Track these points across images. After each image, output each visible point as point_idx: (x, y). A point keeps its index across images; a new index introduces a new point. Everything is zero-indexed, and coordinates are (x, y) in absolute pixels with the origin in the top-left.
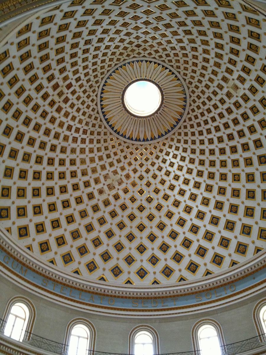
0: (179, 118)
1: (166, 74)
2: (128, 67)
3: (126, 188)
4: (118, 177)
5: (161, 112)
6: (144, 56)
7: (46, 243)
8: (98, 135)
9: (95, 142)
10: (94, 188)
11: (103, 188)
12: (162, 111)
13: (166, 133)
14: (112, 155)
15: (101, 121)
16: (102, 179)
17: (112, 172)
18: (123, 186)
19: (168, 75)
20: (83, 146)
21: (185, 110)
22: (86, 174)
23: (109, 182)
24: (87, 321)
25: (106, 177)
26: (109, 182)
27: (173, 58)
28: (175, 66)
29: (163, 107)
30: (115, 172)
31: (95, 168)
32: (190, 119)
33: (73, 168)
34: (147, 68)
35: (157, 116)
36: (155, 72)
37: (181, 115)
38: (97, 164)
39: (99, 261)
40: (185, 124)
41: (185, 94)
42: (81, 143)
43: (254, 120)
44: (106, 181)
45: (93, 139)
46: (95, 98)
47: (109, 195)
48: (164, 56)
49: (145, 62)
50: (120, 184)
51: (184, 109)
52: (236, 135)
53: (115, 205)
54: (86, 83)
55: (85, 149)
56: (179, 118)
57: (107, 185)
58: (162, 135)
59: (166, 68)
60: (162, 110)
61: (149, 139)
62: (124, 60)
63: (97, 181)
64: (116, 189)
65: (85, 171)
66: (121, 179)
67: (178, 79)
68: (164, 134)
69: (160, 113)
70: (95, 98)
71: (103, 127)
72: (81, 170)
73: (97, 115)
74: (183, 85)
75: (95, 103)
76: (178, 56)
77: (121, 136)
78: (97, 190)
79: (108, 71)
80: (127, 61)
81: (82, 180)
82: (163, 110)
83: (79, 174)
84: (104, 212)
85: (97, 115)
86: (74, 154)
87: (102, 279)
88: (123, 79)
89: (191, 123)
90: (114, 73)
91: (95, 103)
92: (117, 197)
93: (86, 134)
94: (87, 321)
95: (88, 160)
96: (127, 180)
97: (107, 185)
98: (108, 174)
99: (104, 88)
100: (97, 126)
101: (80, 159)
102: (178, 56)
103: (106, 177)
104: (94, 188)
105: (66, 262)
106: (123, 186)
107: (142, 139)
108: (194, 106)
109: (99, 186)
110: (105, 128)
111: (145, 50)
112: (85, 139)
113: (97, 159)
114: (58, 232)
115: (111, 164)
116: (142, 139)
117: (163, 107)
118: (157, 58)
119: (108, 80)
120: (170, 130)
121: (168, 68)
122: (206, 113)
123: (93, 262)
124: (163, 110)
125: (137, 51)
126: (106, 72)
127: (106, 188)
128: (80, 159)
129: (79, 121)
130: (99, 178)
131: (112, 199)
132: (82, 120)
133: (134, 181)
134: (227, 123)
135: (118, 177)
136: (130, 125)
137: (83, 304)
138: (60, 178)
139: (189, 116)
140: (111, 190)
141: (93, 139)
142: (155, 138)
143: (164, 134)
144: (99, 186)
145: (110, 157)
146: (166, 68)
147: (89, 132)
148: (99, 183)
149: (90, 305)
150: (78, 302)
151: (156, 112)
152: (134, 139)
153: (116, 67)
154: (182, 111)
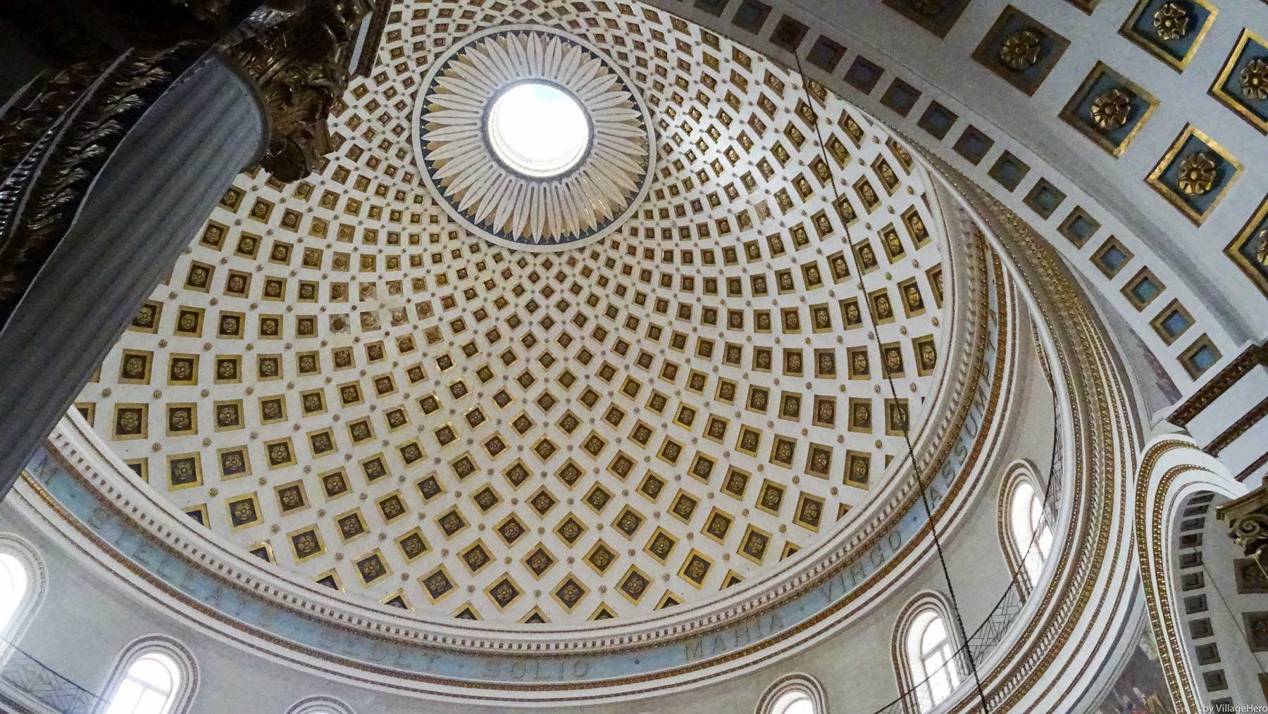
1: (619, 101)
2: (534, 42)
3: (410, 340)
4: (398, 301)
6: (584, 36)
7: (139, 411)
8: (386, 173)
9: (372, 188)
10: (323, 308)
11: (347, 315)
12: (575, 182)
13: (563, 240)
14: (404, 239)
15: (409, 140)
16: (354, 291)
17: (387, 283)
18: (404, 330)
19: (622, 105)
20: (336, 187)
21: (629, 205)
22: (315, 265)
23: (369, 305)
24: (182, 649)
25: (366, 290)
26: (369, 305)
27: (652, 74)
28: (648, 93)
30: (396, 287)
31: (348, 256)
33: (287, 236)
34: (581, 64)
35: (556, 188)
37: (617, 213)
38: (356, 248)
39: (268, 504)
41: (646, 169)
42: (332, 179)
43: (775, 303)
44: (362, 300)
45: (369, 180)
46: (417, 78)
47: (356, 339)
48: (632, 60)
49: (580, 49)
50: (396, 322)
51: (629, 202)
52: (723, 317)
53: (363, 372)
54: (410, 33)
55: (336, 196)
57: (362, 314)
58: (552, 241)
59: (626, 89)
61: (516, 235)
62: (532, 22)
63: (338, 292)
64: (382, 332)
65: (316, 255)
66: (405, 310)
68: (557, 238)
70: (417, 78)
71: (408, 158)
72: (307, 249)
73: (405, 124)
75: (412, 89)
76: (665, 76)
77: (446, 198)
78: (331, 316)
79: (479, 29)
81: (298, 277)
83: (297, 256)
84: (328, 380)
85: (405, 124)
86: (304, 201)
87: (262, 552)
90: (491, 40)
91: (412, 89)
92: (375, 353)
93: (356, 161)
94: (182, 649)
95: (334, 229)
96: (420, 319)
97: (362, 314)
98: (374, 284)
99: (451, 63)
100: (393, 151)
101: (315, 219)
102: (665, 76)
103: (366, 290)
104: (323, 308)
105: (176, 479)
106: (404, 330)
108: (655, 205)
109: (339, 308)
110: (413, 163)
111: (592, 22)
112: (348, 172)
113: (359, 235)
114: (182, 394)
115: (393, 263)
118: (615, 55)
119: (468, 50)
120: (577, 235)
121: (629, 90)
122: (676, 233)
123: (250, 501)
125: (572, 17)
126: (472, 28)
127: (355, 320)
128: (315, 219)
129: (352, 119)
130: (346, 285)
131: (360, 354)
132: (359, 119)
133: (436, 328)
134: (714, 281)
135: (398, 301)
137: (188, 602)
138: (240, 250)
139: (634, 223)
140: (368, 330)
141: (369, 180)
142: (530, 241)
143: (557, 238)
144: (339, 308)
145: (397, 242)
146: (626, 89)
147: (365, 157)
148: (341, 301)
149: (205, 611)
150: (174, 594)
151: (560, 178)
152: (478, 220)
153: (503, 28)
154: (624, 204)
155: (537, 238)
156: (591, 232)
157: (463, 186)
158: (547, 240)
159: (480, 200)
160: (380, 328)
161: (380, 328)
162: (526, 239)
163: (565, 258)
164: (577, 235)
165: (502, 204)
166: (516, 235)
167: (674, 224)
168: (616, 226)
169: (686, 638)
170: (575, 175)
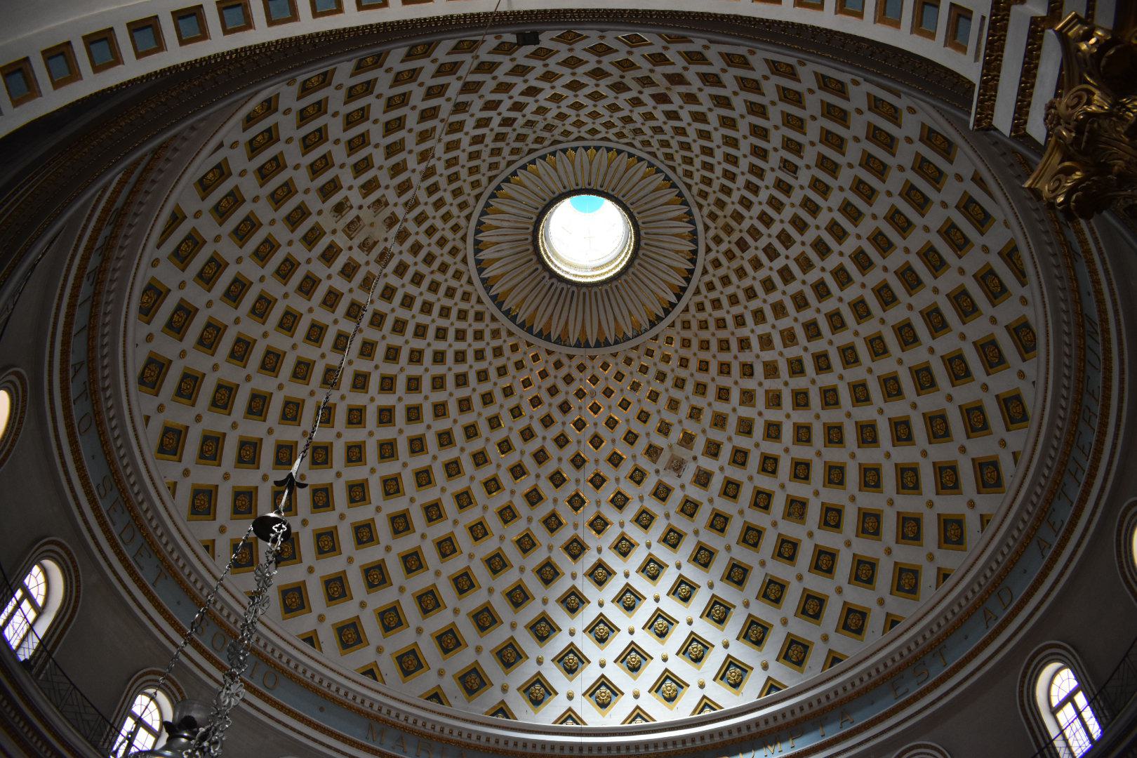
0: (554, 337)
5: (557, 288)
11: (351, 207)
13: (507, 313)
29: (568, 289)
32: (558, 365)
34: (677, 252)
35: (544, 278)
36: (663, 267)
40: (543, 356)
41: (616, 342)
44: (369, 207)
56: (554, 337)
58: (499, 305)
60: (563, 289)
64: (350, 243)
66: (375, 243)
67: (652, 324)
68: (505, 307)
69: (552, 284)
74: (638, 335)
80: (695, 210)
82: (561, 292)
88: (642, 194)
89: (551, 371)
97: (358, 217)
98: (387, 204)
107: (481, 256)
116: (481, 256)
117: (568, 289)
124: (561, 292)
127: (350, 216)
136: (513, 218)
143: (505, 307)
152: (480, 237)
154: (573, 341)
155: (493, 292)
156: (530, 330)
157: (504, 208)
158: (498, 301)
159: (497, 228)
160: (351, 239)
161: (351, 239)
162: (487, 284)
163: (494, 326)
164: (519, 321)
165: (504, 246)
166: (485, 275)
167: (593, 394)
168: (552, 347)
169: (377, 719)
170: (564, 285)
